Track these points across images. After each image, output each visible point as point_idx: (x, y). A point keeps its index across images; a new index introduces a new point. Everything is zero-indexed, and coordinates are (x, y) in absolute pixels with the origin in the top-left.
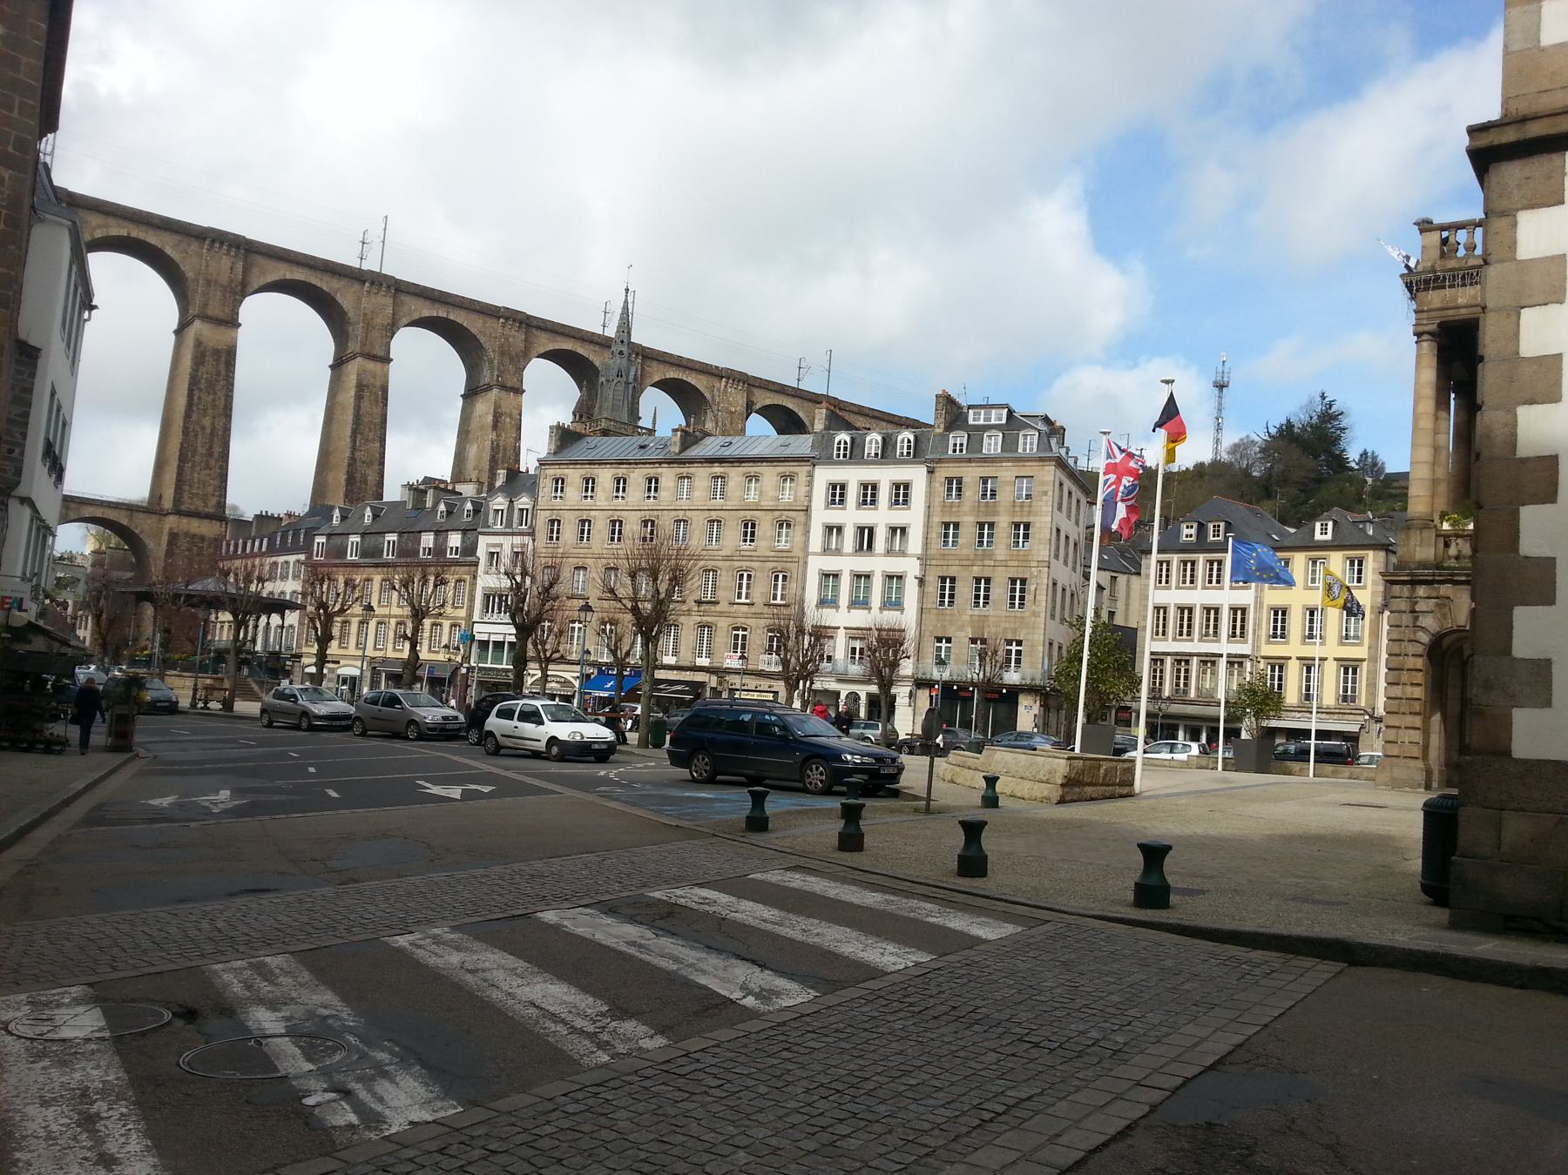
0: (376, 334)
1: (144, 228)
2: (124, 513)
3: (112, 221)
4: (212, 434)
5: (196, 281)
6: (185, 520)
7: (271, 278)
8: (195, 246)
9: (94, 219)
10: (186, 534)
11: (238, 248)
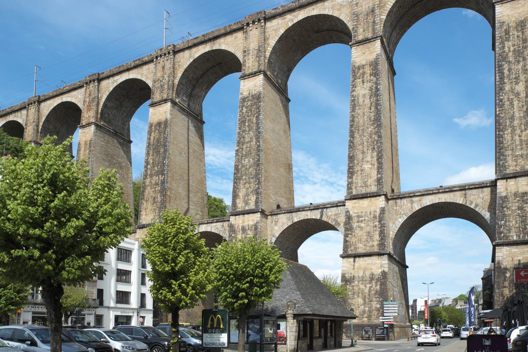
6: (512, 182)
10: (516, 195)
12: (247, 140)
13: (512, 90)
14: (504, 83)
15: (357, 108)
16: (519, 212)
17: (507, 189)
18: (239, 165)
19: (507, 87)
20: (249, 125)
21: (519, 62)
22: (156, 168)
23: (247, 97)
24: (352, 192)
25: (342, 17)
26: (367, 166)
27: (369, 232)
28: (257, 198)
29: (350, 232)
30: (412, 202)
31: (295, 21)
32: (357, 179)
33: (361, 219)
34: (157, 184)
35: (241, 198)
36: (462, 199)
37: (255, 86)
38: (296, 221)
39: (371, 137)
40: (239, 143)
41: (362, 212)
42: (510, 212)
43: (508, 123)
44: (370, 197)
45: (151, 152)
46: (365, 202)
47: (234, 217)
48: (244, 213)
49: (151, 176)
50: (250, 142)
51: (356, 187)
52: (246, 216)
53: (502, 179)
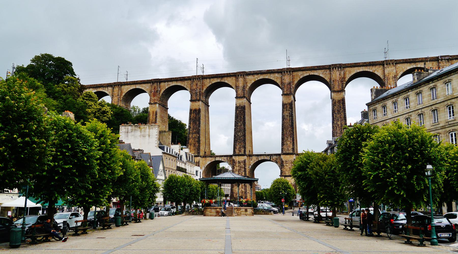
0: (391, 80)
1: (313, 71)
3: (304, 72)
5: (330, 81)
7: (352, 74)
9: (300, 73)
11: (341, 68)
12: (239, 124)
13: (337, 123)
25: (278, 82)
26: (288, 143)
32: (285, 147)
40: (235, 126)
46: (288, 156)
48: (239, 155)
49: (192, 133)
50: (241, 126)
52: (240, 157)
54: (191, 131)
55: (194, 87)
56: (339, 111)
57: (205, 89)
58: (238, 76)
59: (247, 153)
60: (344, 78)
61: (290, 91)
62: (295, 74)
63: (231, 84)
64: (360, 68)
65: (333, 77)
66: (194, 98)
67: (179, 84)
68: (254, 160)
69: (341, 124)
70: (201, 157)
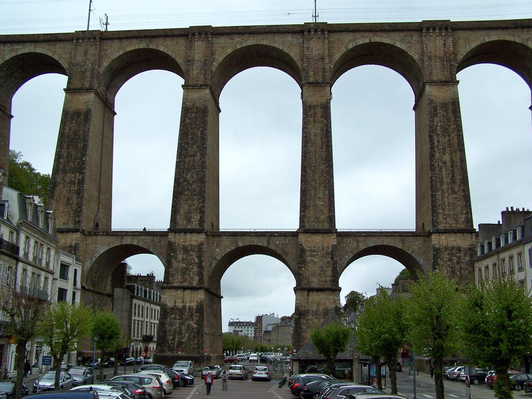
1: (379, 34)
2: (398, 239)
3: (358, 35)
4: (452, 166)
6: (443, 237)
8: (416, 36)
9: (347, 37)
11: (446, 29)
14: (435, 151)
15: (309, 145)
16: (450, 263)
17: (439, 243)
18: (180, 179)
19: (437, 156)
20: (192, 139)
21: (445, 136)
22: (72, 164)
23: (191, 109)
24: (304, 226)
25: (292, 54)
26: (320, 203)
27: (322, 267)
28: (201, 217)
29: (303, 266)
30: (358, 242)
31: (244, 45)
32: (311, 213)
33: (314, 253)
34: (72, 183)
35: (182, 214)
36: (401, 244)
37: (200, 98)
38: (241, 246)
39: (322, 175)
41: (315, 247)
42: (442, 263)
43: (438, 186)
44: (323, 233)
45: (65, 145)
46: (318, 238)
47: (173, 234)
48: (186, 231)
49: (65, 172)
50: (194, 156)
51: (308, 221)
52: (188, 236)
53: (436, 233)
54: (61, 166)
55: (79, 58)
56: (445, 130)
57: (105, 64)
58: (194, 34)
59: (207, 226)
60: (455, 54)
61: (324, 77)
62: (334, 37)
63: (173, 56)
64: (491, 32)
65: (429, 49)
66: (77, 84)
67: (40, 49)
68: (228, 246)
69: (452, 161)
70: (83, 232)
